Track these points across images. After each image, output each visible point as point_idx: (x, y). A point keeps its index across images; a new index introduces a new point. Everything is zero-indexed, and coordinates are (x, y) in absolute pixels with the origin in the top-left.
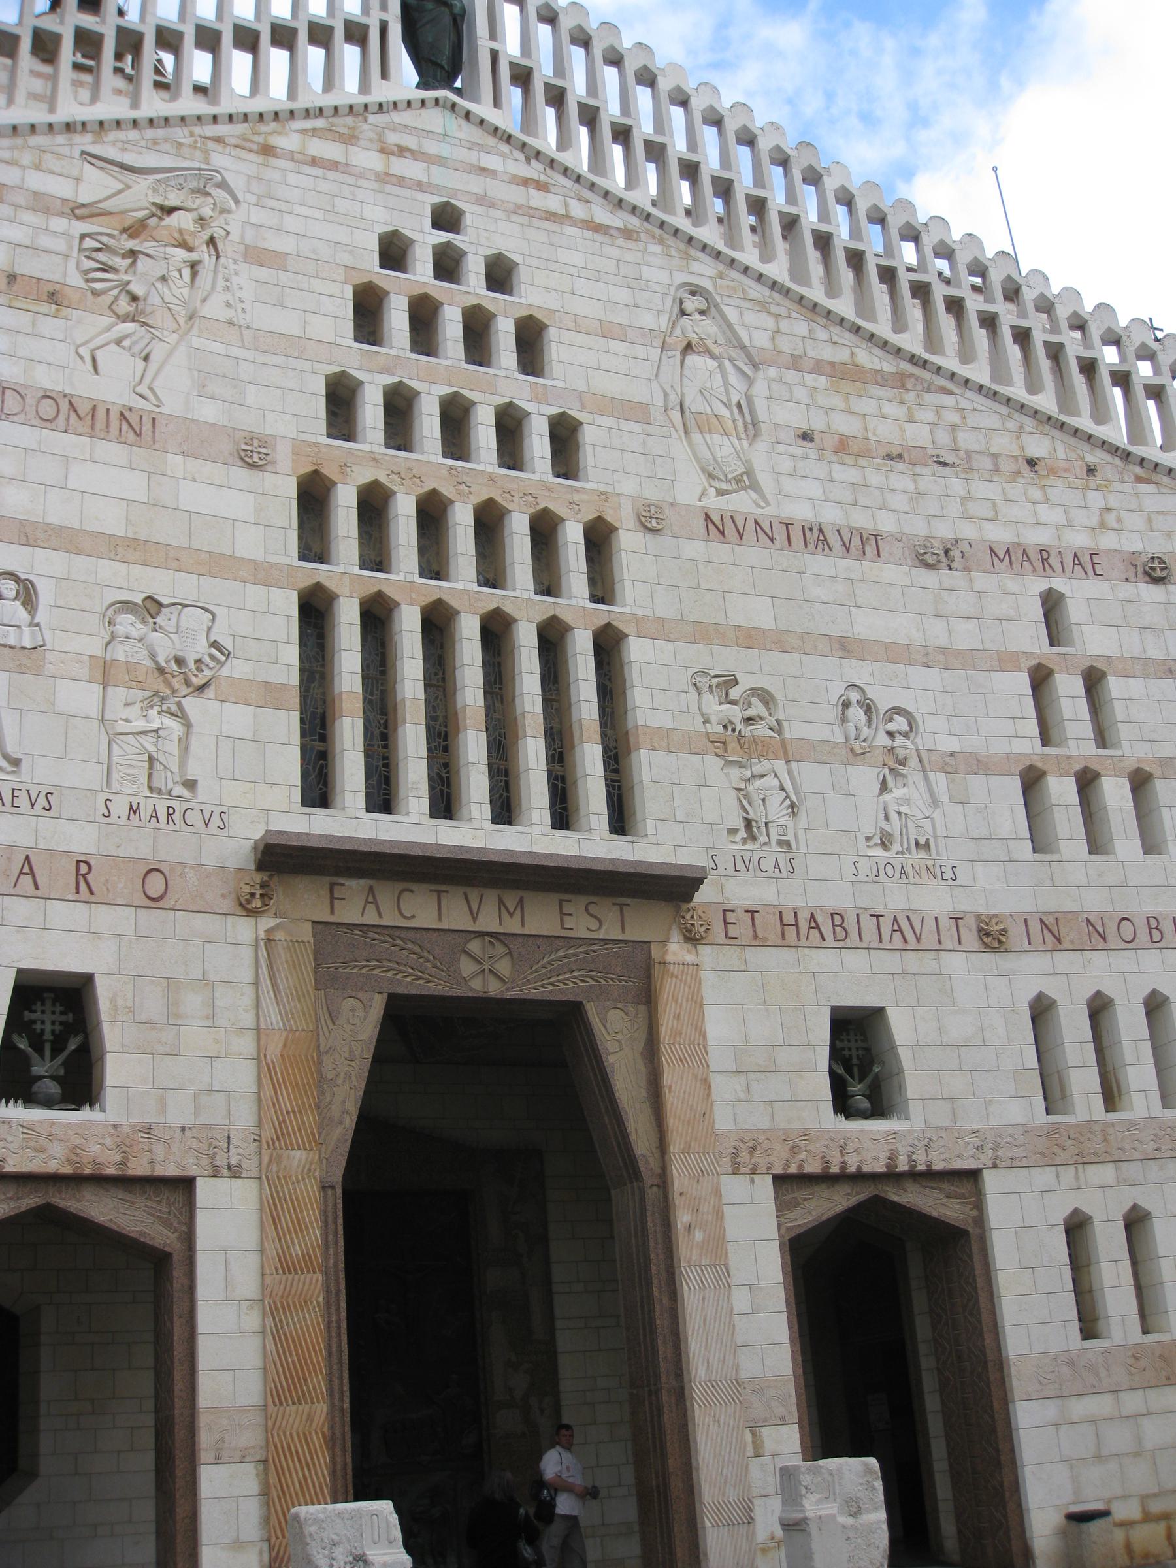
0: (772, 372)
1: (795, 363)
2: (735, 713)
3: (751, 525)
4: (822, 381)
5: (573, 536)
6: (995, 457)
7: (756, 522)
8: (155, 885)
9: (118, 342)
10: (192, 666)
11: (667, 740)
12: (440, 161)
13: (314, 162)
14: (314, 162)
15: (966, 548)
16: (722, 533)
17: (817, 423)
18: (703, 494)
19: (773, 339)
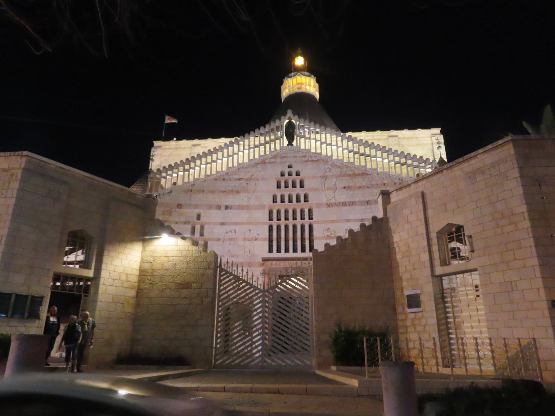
0: (340, 178)
1: (343, 176)
2: (329, 234)
3: (334, 204)
4: (348, 177)
5: (306, 211)
6: (377, 185)
7: (335, 204)
8: (250, 265)
9: (246, 196)
10: (255, 237)
11: (319, 238)
12: (289, 157)
13: (271, 163)
14: (271, 163)
15: (370, 201)
16: (329, 206)
17: (346, 185)
18: (327, 201)
19: (340, 172)
